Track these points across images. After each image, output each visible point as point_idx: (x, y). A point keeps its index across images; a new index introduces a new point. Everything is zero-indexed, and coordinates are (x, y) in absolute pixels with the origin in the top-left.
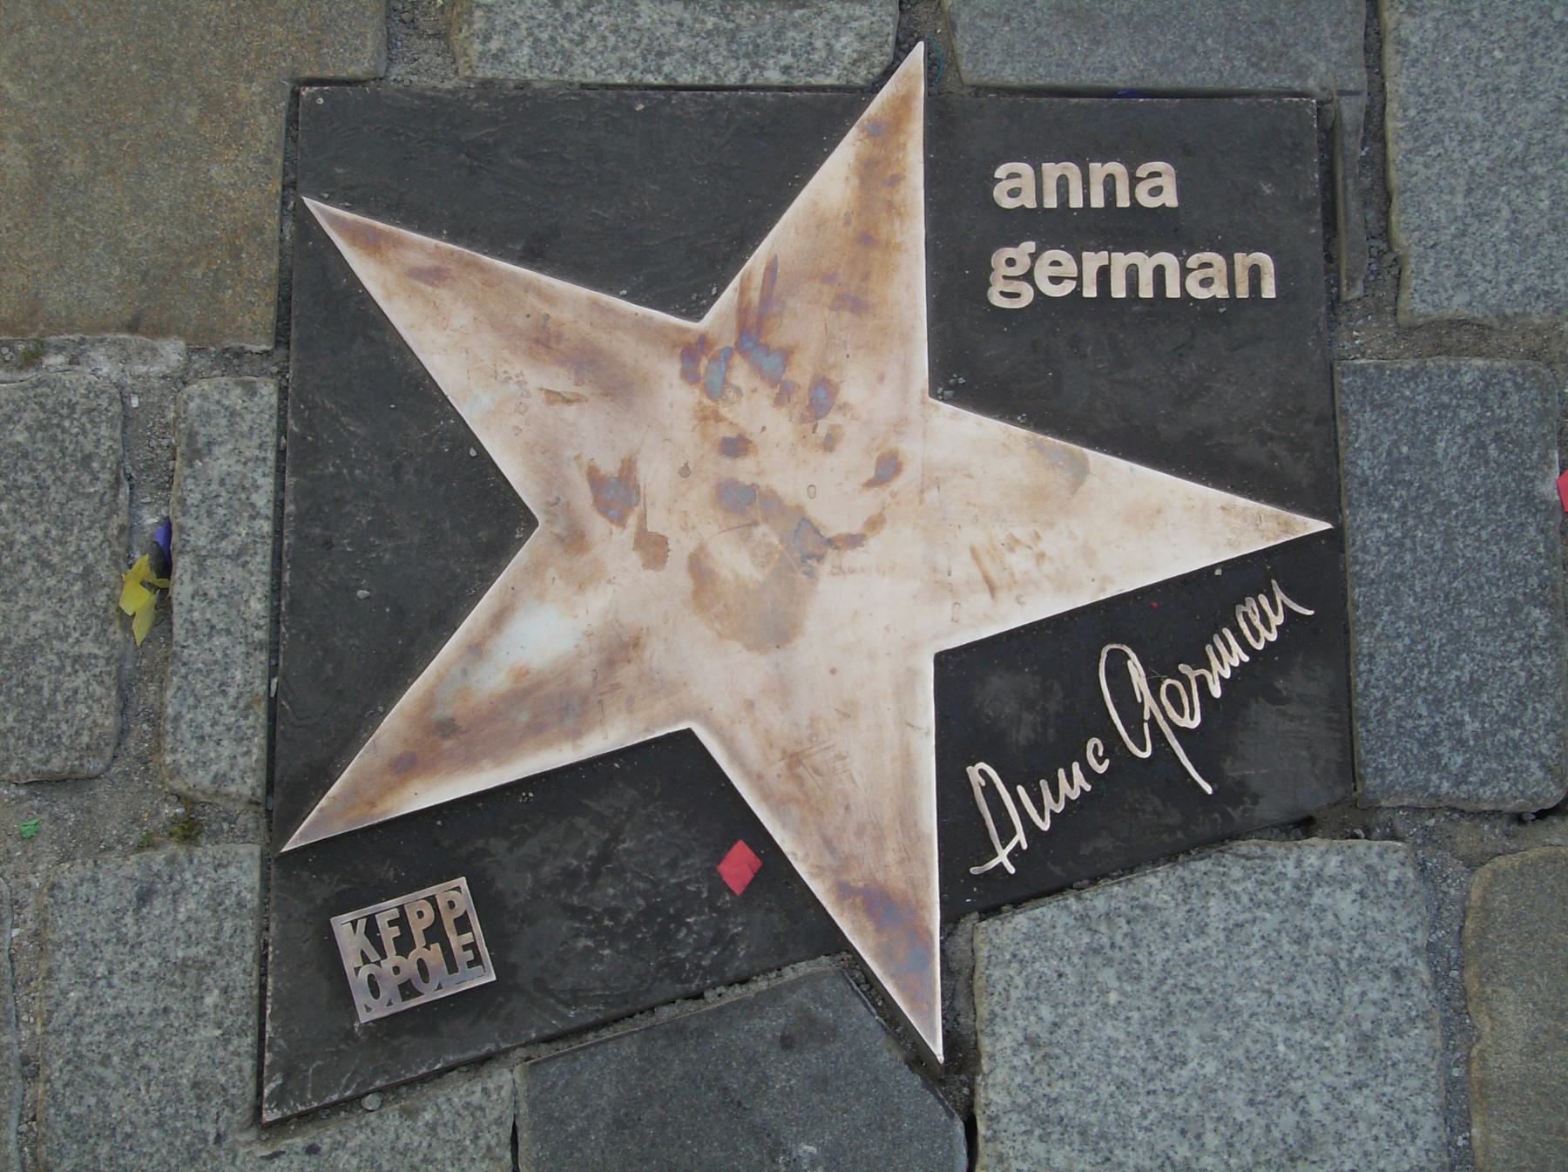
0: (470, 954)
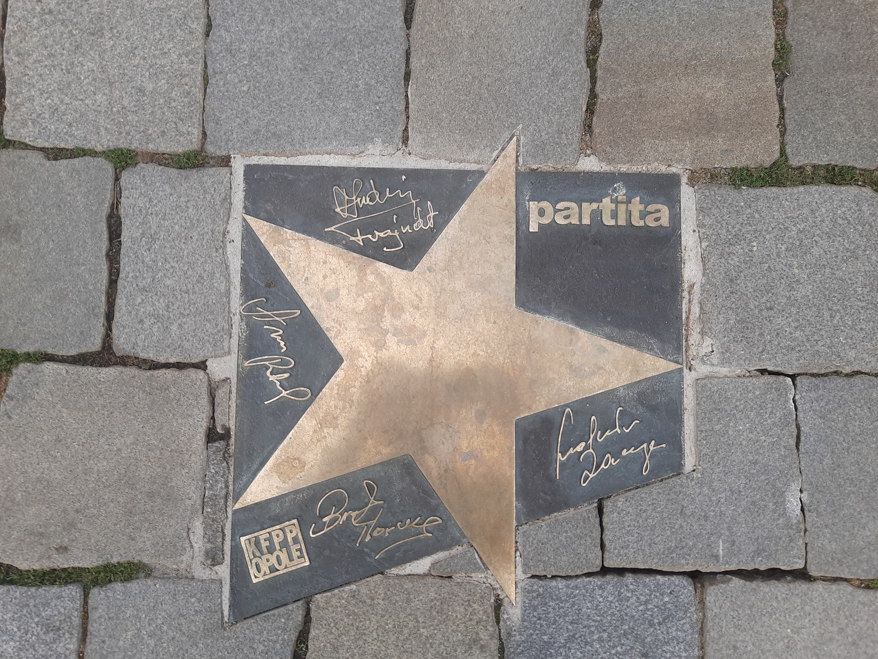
0: (298, 553)
